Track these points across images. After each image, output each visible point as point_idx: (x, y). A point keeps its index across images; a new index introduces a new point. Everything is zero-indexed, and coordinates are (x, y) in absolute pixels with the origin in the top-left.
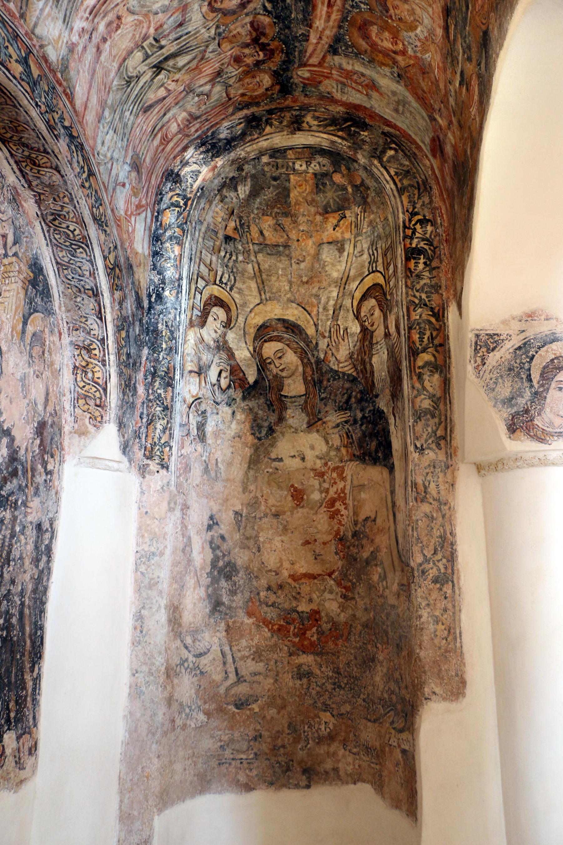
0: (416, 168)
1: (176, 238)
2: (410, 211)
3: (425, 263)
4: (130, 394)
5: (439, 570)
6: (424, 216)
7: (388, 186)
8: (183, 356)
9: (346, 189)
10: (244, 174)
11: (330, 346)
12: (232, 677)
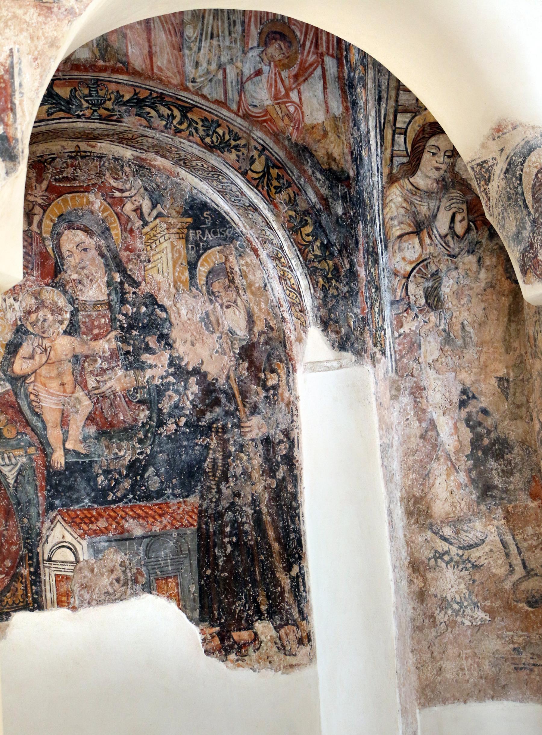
12: (519, 571)
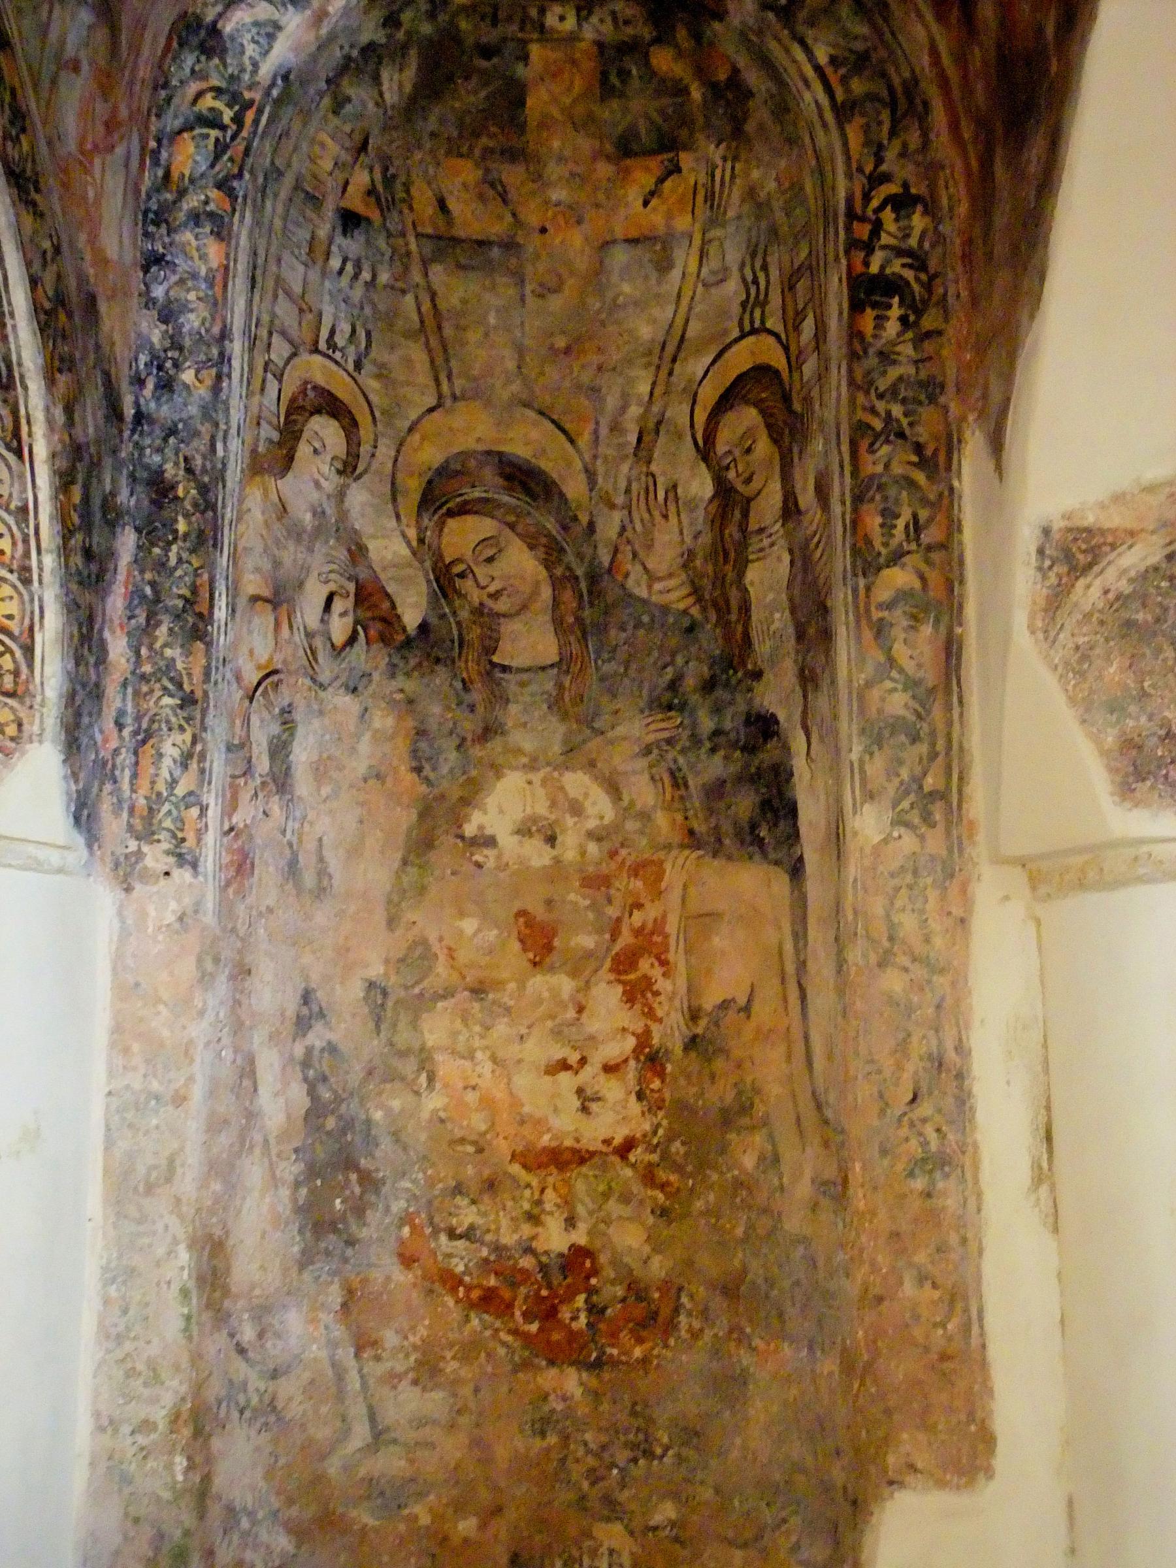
0: (886, 45)
1: (211, 215)
2: (868, 169)
3: (903, 320)
4: (92, 660)
5: (925, 1144)
6: (906, 186)
7: (807, 96)
8: (234, 557)
9: (685, 91)
10: (400, 35)
11: (629, 534)
12: (361, 1434)
